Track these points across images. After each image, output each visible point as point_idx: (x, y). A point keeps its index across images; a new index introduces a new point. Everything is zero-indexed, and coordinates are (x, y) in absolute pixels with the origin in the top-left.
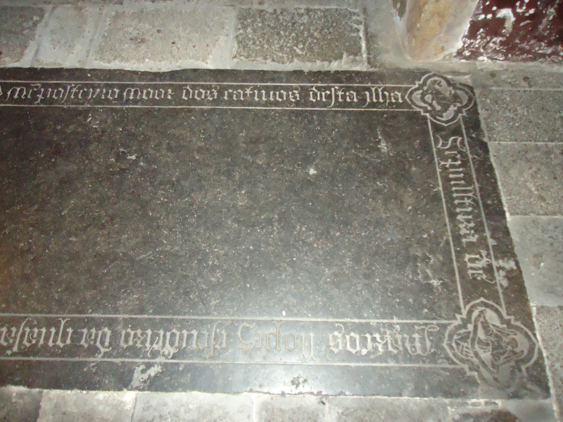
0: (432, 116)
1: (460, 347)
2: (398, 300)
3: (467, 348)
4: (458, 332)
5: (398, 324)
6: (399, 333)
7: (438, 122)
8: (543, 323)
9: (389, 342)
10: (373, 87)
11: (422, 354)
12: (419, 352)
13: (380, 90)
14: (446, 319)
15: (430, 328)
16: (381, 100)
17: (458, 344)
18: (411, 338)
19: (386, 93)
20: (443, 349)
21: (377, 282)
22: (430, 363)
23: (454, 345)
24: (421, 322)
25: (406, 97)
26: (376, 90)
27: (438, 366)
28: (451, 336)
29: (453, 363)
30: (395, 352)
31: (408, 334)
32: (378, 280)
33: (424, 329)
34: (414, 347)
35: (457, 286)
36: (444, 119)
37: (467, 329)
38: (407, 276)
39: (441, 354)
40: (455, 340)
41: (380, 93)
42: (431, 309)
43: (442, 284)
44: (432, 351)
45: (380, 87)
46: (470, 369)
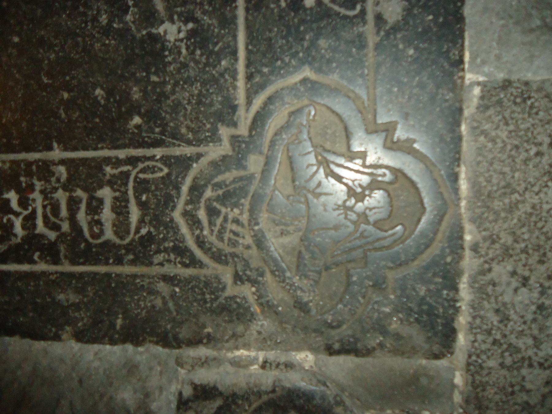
1: (219, 221)
2: (66, 95)
3: (236, 221)
4: (216, 180)
5: (62, 162)
6: (65, 189)
8: (493, 141)
9: (40, 211)
11: (118, 241)
12: (109, 234)
14: (189, 143)
15: (143, 171)
17: (212, 212)
18: (92, 198)
20: (172, 226)
21: (15, 45)
22: (133, 263)
23: (202, 214)
24: (122, 154)
27: (155, 270)
28: (196, 190)
29: (194, 262)
30: (52, 235)
31: (85, 189)
32: (16, 39)
33: (127, 175)
34: (99, 223)
35: (235, 37)
37: (245, 168)
38: (95, 19)
39: (165, 239)
40: (209, 199)
42: (152, 116)
43: (192, 34)
44: (144, 231)
46: (238, 278)
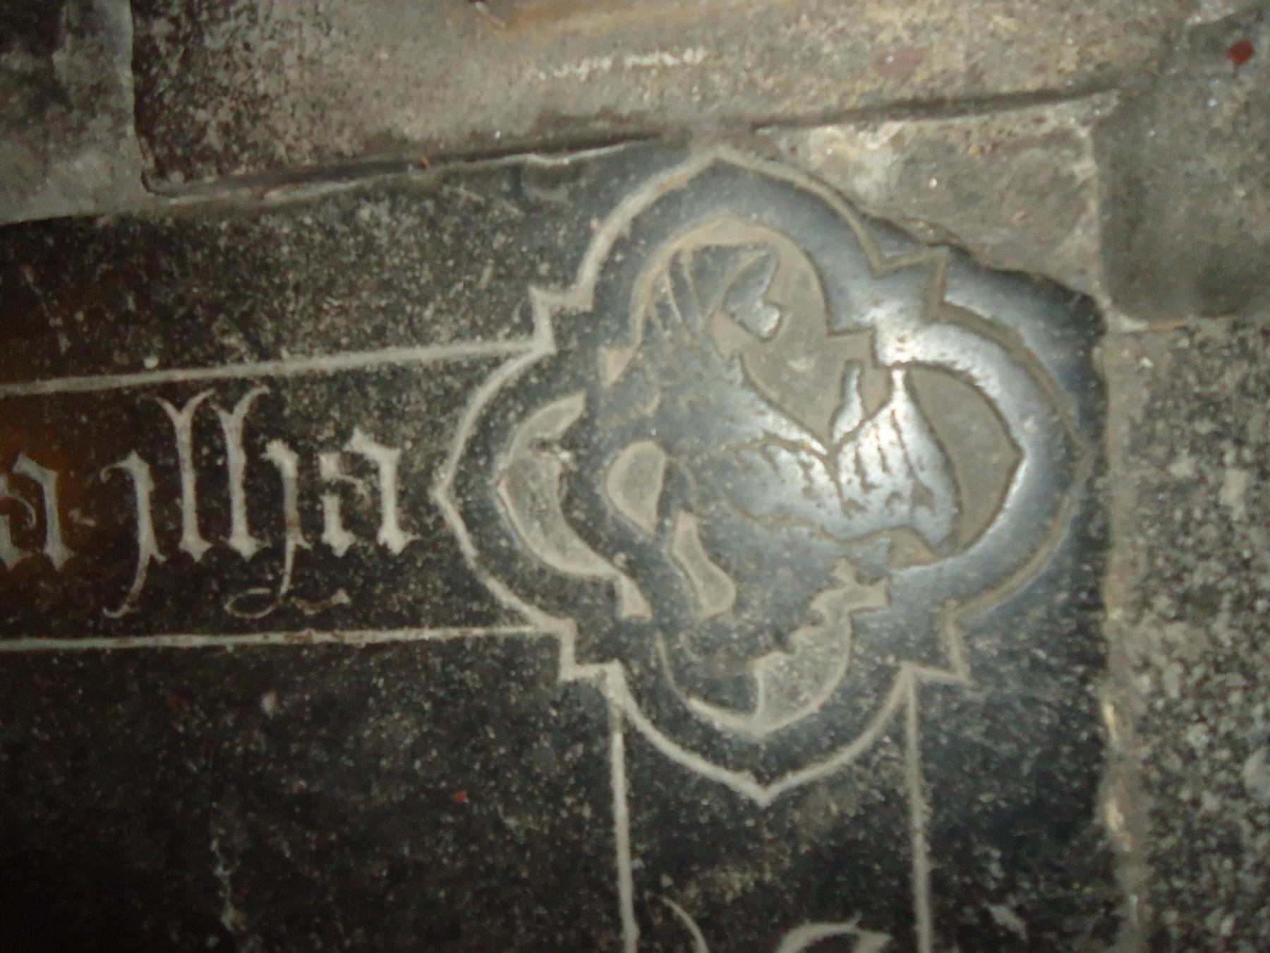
0: (646, 691)
7: (700, 765)
10: (178, 394)
13: (232, 424)
16: (243, 542)
19: (281, 455)
25: (441, 494)
26: (206, 430)
36: (758, 725)
41: (237, 459)
45: (229, 391)
